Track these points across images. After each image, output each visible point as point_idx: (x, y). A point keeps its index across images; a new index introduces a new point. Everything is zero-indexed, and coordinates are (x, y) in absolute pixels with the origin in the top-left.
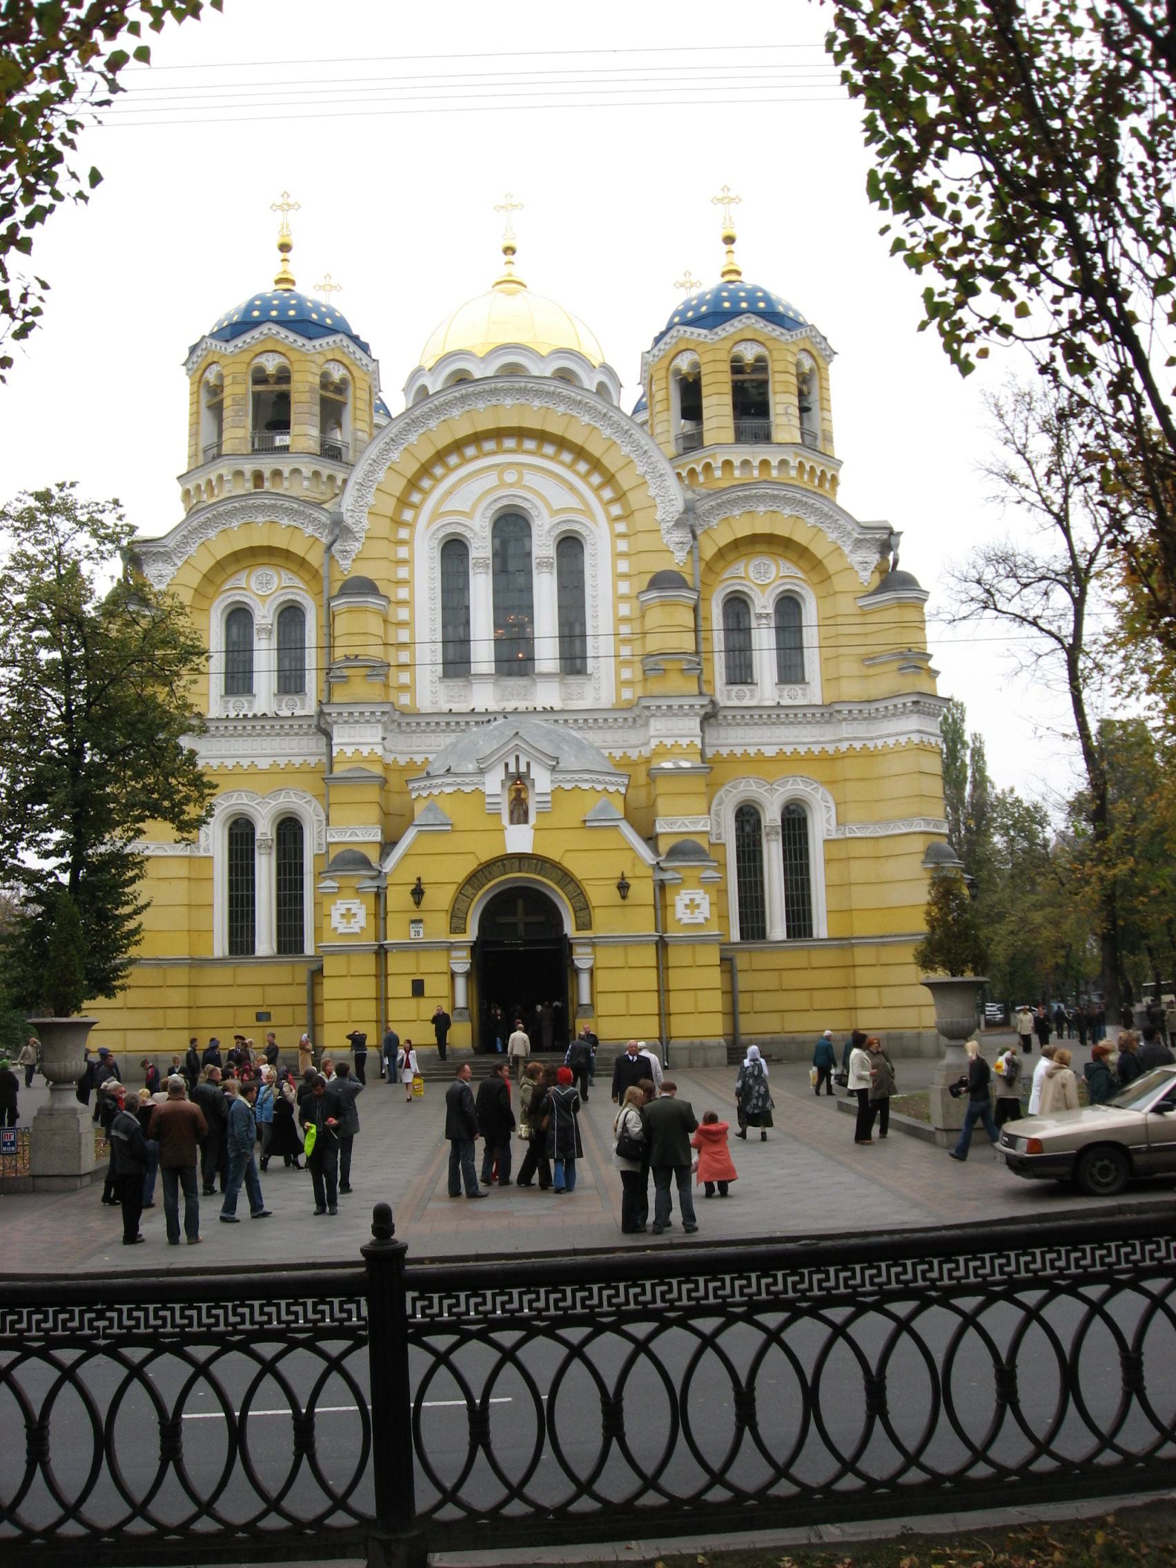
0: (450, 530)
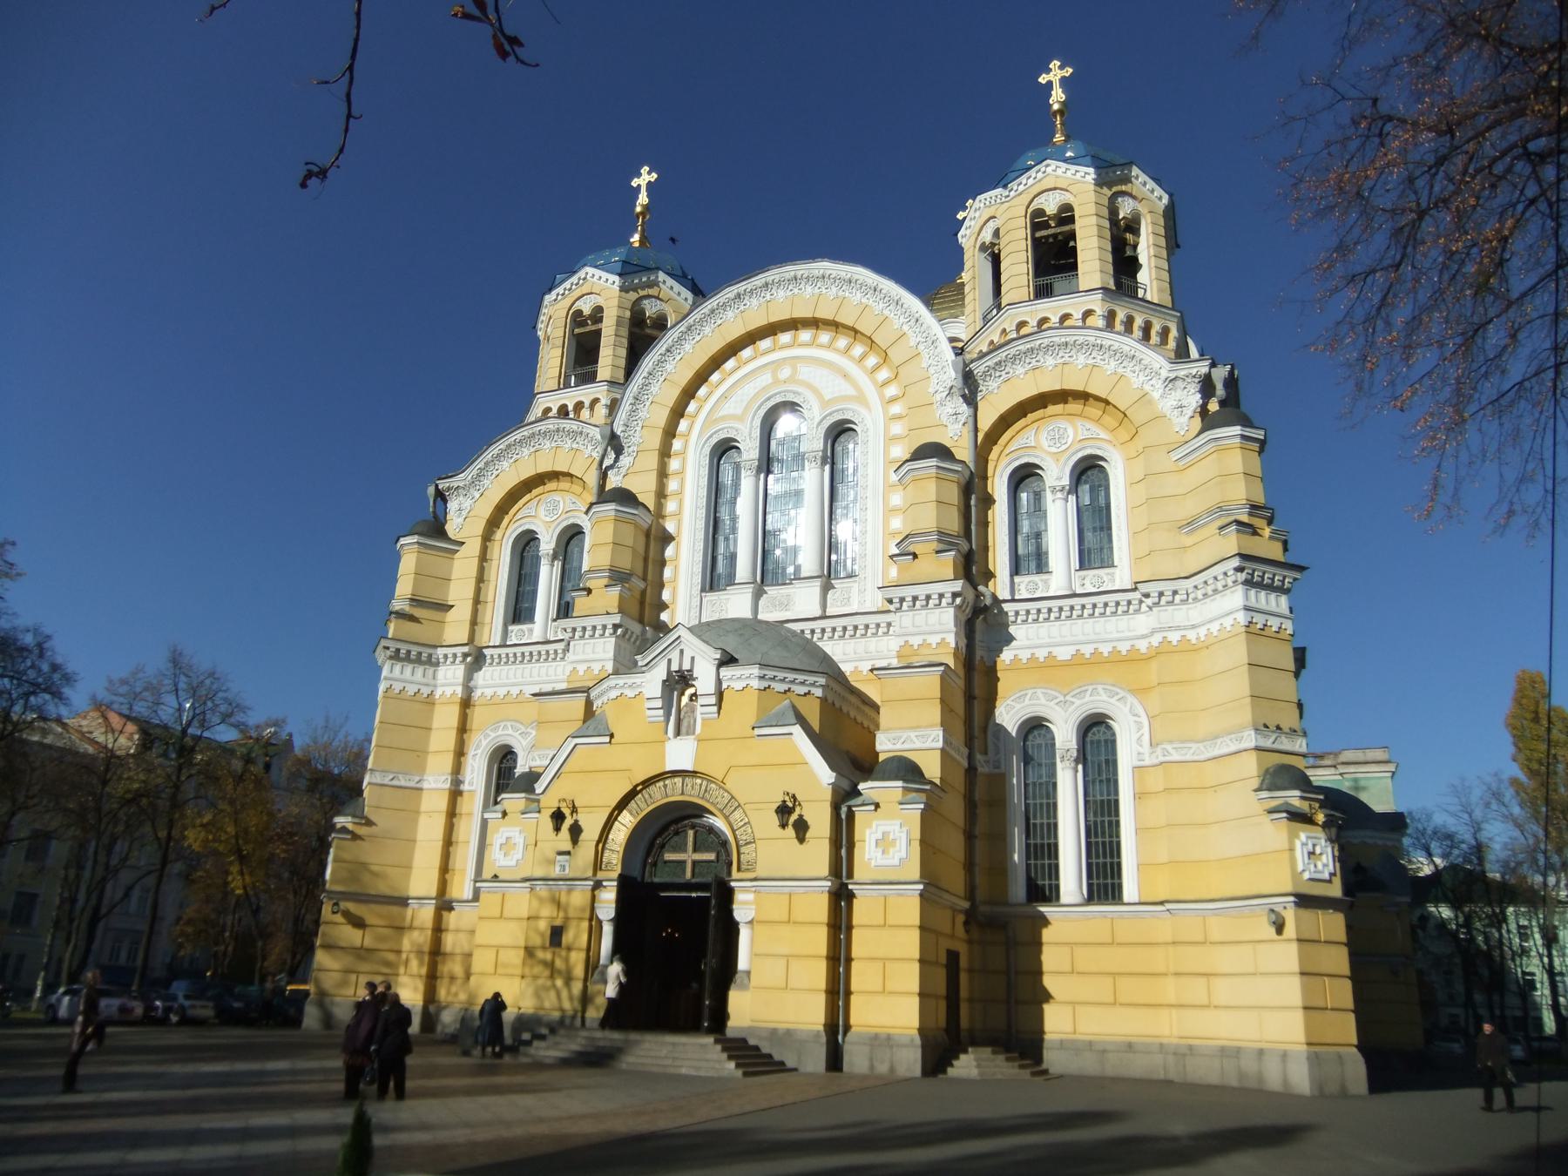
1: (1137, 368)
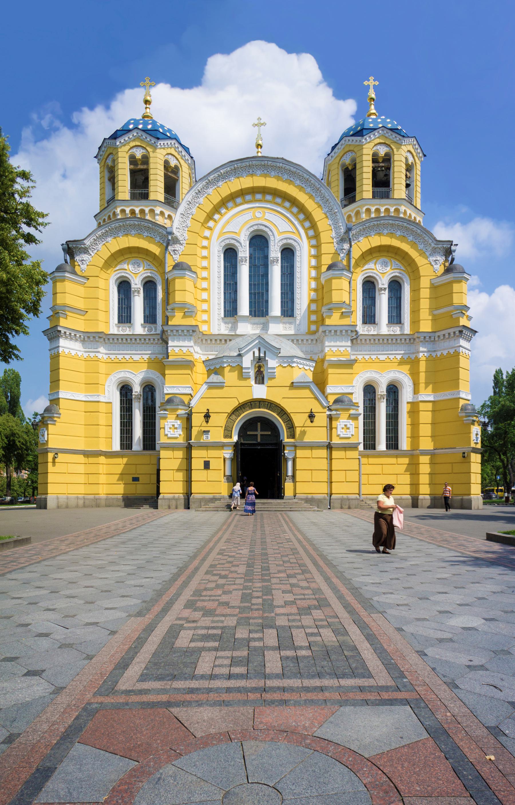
0: (227, 242)
1: (422, 241)
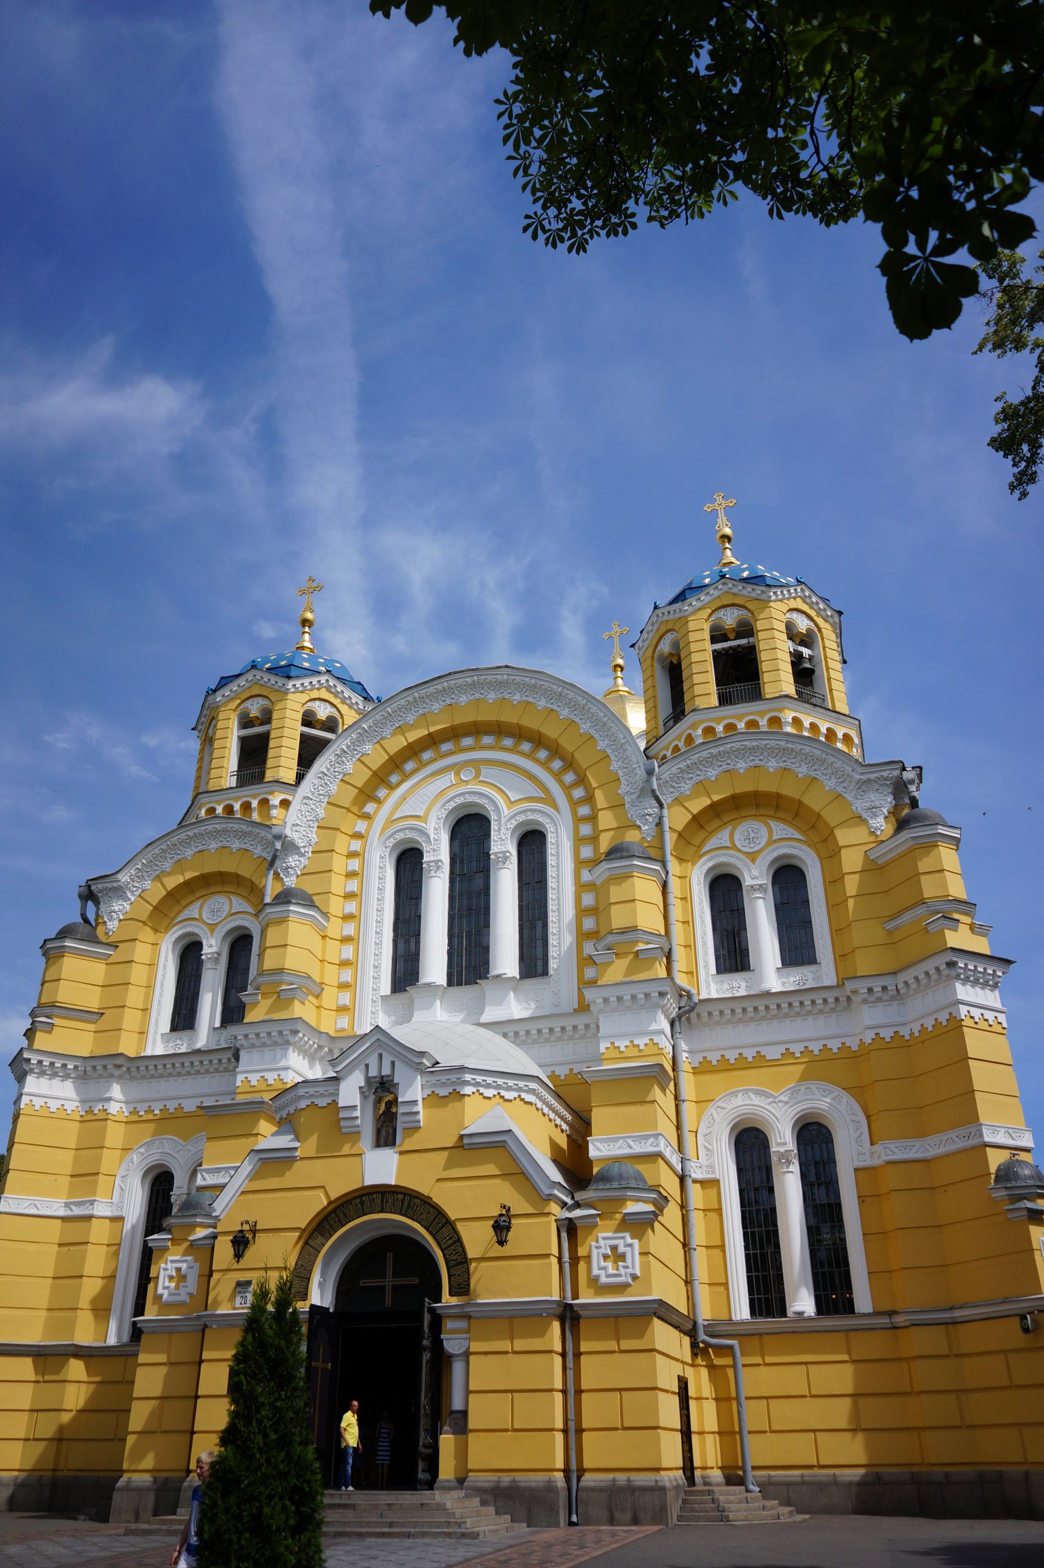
0: (400, 836)
1: (829, 771)
